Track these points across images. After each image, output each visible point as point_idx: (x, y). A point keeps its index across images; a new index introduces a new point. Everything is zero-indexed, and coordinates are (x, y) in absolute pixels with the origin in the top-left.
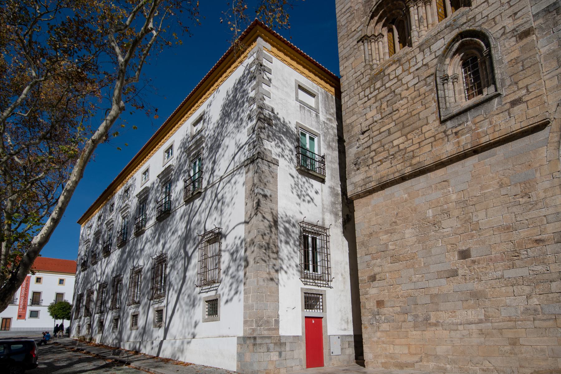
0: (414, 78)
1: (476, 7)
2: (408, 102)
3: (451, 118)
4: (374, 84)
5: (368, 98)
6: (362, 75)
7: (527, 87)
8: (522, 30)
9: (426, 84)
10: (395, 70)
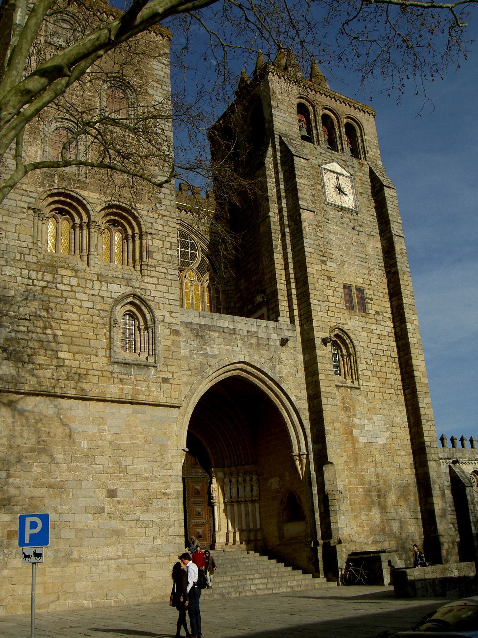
0: (88, 301)
1: (148, 283)
2: (80, 321)
3: (119, 363)
4: (44, 272)
5: (33, 282)
6: (27, 251)
9: (99, 316)
10: (70, 277)
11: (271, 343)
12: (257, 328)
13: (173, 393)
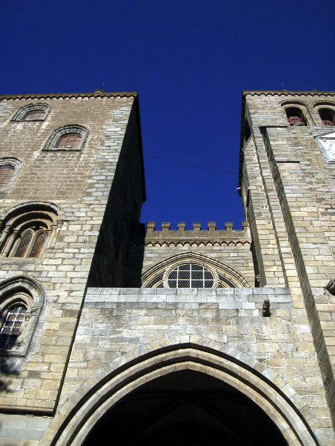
1: (47, 265)
7: (50, 364)
8: (70, 308)
11: (242, 314)
12: (217, 299)
13: (41, 391)
